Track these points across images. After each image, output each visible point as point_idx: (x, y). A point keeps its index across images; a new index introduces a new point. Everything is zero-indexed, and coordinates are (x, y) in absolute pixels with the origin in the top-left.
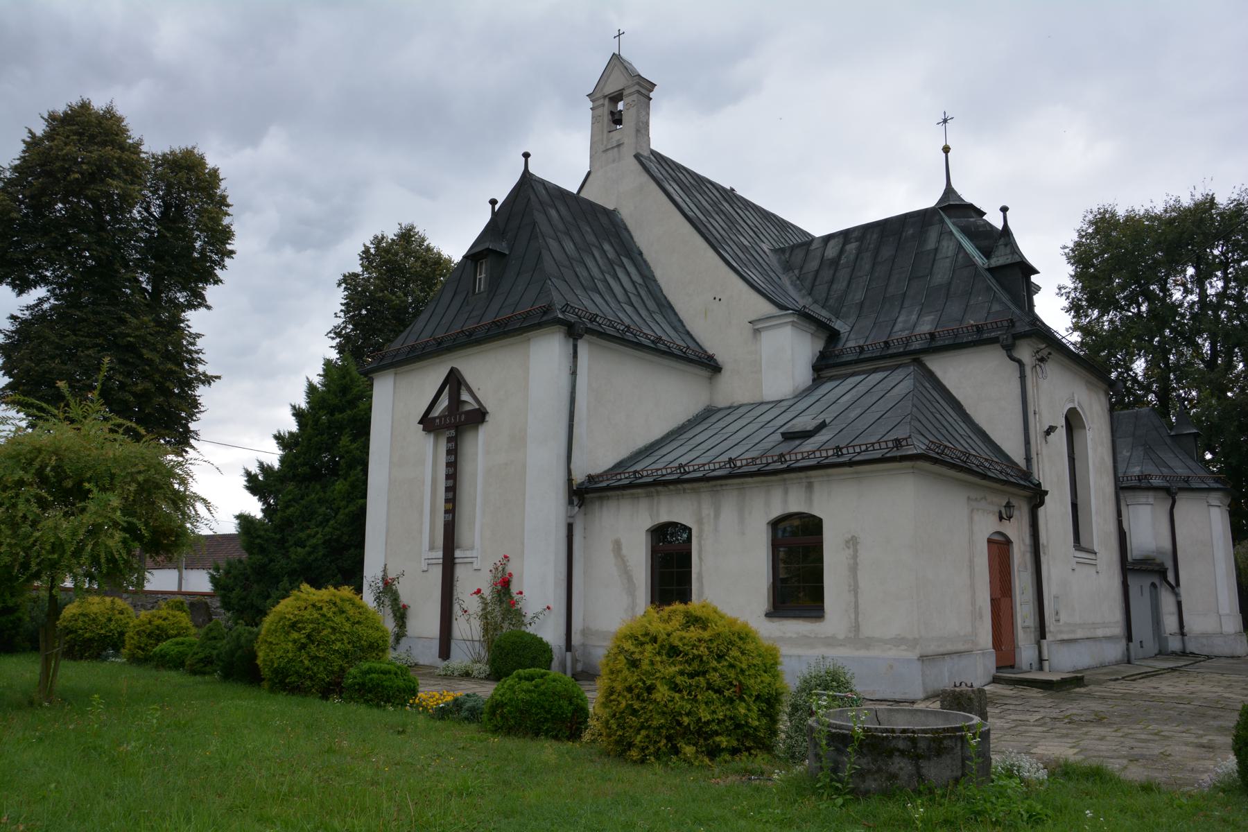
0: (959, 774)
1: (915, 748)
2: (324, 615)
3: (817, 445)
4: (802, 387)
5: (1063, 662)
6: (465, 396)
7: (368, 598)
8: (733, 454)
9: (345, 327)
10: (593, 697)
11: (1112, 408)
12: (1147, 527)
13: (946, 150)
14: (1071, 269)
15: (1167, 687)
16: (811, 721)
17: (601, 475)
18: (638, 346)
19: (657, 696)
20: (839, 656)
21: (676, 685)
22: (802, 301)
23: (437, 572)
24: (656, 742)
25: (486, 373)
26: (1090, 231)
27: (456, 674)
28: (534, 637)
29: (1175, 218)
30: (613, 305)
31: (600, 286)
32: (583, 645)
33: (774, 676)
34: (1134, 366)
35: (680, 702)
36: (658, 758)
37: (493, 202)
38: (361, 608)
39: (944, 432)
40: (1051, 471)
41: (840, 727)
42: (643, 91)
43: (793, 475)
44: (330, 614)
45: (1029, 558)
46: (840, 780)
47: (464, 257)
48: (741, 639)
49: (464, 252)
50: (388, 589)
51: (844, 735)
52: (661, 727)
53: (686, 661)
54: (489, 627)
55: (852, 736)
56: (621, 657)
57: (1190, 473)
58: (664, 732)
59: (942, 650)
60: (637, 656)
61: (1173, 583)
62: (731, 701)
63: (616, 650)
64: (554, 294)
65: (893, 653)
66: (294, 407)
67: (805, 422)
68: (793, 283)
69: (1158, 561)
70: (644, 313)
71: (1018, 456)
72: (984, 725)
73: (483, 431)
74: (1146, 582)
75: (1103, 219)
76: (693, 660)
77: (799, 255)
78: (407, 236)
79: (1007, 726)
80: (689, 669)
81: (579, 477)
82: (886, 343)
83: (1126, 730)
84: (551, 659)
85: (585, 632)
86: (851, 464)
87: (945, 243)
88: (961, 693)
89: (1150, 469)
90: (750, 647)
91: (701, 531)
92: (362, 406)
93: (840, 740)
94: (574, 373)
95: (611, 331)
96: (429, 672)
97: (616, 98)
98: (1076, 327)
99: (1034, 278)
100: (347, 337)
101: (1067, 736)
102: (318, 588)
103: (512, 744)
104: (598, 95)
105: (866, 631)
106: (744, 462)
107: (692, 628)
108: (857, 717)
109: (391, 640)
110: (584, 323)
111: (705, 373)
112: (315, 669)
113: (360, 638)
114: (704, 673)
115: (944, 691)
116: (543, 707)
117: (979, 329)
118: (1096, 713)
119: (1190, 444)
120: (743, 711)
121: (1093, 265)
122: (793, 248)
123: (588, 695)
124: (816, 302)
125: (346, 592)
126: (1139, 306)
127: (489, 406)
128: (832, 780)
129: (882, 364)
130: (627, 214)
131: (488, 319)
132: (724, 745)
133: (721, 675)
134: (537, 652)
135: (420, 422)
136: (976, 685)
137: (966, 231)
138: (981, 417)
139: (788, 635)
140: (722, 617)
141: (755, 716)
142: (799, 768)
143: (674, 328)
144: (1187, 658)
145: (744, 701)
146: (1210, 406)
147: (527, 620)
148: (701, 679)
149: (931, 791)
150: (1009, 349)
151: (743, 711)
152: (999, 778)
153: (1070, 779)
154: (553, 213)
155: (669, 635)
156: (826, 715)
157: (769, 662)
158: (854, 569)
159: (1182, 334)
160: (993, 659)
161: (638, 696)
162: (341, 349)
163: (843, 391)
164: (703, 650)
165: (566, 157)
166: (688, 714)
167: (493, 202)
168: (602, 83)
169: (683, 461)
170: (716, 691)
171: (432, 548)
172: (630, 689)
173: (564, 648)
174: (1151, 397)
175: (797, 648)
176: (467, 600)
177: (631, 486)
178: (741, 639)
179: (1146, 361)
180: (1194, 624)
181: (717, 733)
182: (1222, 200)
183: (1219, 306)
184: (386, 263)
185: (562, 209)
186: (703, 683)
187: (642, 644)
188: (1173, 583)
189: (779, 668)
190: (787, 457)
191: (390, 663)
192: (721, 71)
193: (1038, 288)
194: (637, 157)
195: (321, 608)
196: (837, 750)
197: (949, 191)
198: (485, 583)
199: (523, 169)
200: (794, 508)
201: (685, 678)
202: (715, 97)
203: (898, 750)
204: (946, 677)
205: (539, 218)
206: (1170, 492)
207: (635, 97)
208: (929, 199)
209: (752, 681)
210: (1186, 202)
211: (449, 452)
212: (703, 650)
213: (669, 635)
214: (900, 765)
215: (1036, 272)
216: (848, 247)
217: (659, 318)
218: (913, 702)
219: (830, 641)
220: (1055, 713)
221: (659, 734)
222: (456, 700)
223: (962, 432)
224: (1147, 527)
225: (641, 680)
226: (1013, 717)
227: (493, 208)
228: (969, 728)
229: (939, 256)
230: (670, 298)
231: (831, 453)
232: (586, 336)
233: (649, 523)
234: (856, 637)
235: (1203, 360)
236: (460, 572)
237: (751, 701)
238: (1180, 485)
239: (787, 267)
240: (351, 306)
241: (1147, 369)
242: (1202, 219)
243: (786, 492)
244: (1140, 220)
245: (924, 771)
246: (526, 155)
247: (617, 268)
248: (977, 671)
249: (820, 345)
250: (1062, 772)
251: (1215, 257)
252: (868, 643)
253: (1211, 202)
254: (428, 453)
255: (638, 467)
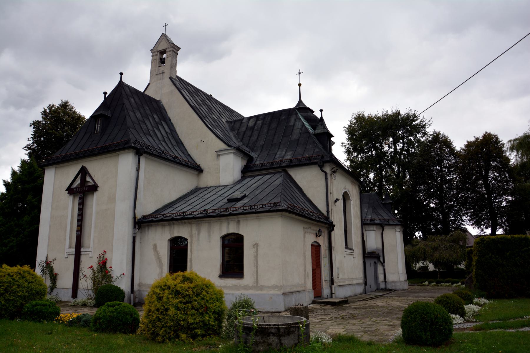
0: (297, 342)
1: (279, 332)
2: (14, 279)
3: (242, 204)
4: (237, 180)
5: (341, 294)
6: (88, 179)
7: (38, 271)
8: (207, 207)
9: (33, 145)
10: (142, 314)
11: (361, 192)
12: (373, 240)
13: (300, 85)
14: (346, 136)
15: (379, 303)
16: (236, 322)
17: (148, 216)
18: (167, 160)
19: (170, 313)
20: (249, 294)
21: (178, 308)
22: (238, 144)
23: (72, 258)
24: (169, 333)
25: (99, 169)
26: (354, 121)
27: (80, 304)
28: (116, 287)
29: (386, 118)
30: (157, 142)
31: (151, 133)
32: (139, 291)
33: (221, 303)
34: (370, 176)
35: (180, 315)
36: (170, 340)
37: (105, 93)
38: (34, 276)
39: (294, 200)
40: (337, 217)
41: (248, 324)
42: (175, 50)
43: (232, 217)
44: (17, 279)
45: (327, 252)
46: (248, 347)
47: (91, 117)
48: (207, 287)
49: (91, 114)
50: (48, 266)
51: (249, 327)
52: (172, 326)
53: (183, 297)
54: (96, 282)
55: (253, 328)
56: (154, 296)
57: (389, 219)
58: (173, 328)
59: (292, 290)
60: (161, 295)
61: (382, 261)
62: (202, 314)
63: (152, 293)
64: (131, 135)
65: (272, 292)
66: (4, 181)
67: (238, 195)
68: (234, 136)
69: (377, 253)
70: (170, 146)
71: (323, 210)
72: (307, 321)
73: (96, 195)
74: (372, 261)
75: (359, 117)
76: (186, 296)
77: (237, 125)
78: (65, 105)
79: (318, 321)
80: (184, 300)
81: (139, 216)
82: (272, 163)
83: (363, 321)
84: (124, 297)
85: (140, 285)
86: (256, 213)
87: (297, 123)
88: (298, 308)
89: (375, 217)
90: (211, 290)
91: (192, 240)
92: (39, 182)
93: (248, 329)
94: (138, 170)
95: (155, 153)
96: (66, 304)
97: (163, 52)
98: (348, 159)
99: (332, 139)
100: (33, 150)
101: (340, 324)
102: (12, 266)
103: (104, 336)
104: (155, 50)
105: (261, 283)
106: (211, 211)
107: (186, 283)
108: (255, 320)
109: (48, 290)
110: (143, 149)
111: (196, 173)
112: (8, 305)
113: (32, 290)
114: (190, 302)
115: (291, 308)
116: (119, 319)
117: (310, 158)
118: (352, 314)
119: (389, 207)
120: (207, 318)
121: (355, 135)
122: (235, 121)
123: (140, 313)
124: (244, 144)
125: (26, 268)
126: (372, 152)
127: (99, 183)
128: (244, 347)
129: (270, 171)
130: (165, 103)
131: (100, 145)
132: (199, 333)
133: (198, 303)
134: (118, 294)
135: (66, 190)
136: (305, 305)
137: (306, 118)
138: (309, 195)
139: (228, 285)
140: (199, 278)
141: (212, 320)
142: (231, 342)
143: (183, 153)
144: (387, 291)
145: (208, 314)
146: (397, 192)
147: (113, 280)
148: (189, 305)
149: (285, 350)
150: (321, 167)
151: (207, 318)
152: (313, 343)
153: (341, 342)
154: (132, 100)
155: (175, 286)
156: (243, 319)
157: (219, 296)
158: (256, 257)
159: (387, 164)
160: (313, 294)
161: (162, 313)
162: (30, 155)
163: (253, 182)
164: (190, 292)
165: (139, 76)
166: (183, 320)
167: (105, 93)
168: (158, 43)
169: (185, 210)
170: (196, 310)
171: (70, 247)
172: (158, 310)
173: (130, 292)
174: (376, 188)
175: (231, 291)
176: (86, 270)
177: (162, 220)
178: (207, 287)
179: (374, 174)
180: (390, 278)
181: (196, 328)
182: (403, 113)
183: (401, 154)
184: (54, 117)
185: (136, 99)
186: (190, 307)
187: (164, 290)
188: (382, 261)
189: (223, 299)
190: (229, 209)
191: (47, 300)
192: (212, 46)
193: (334, 143)
194: (171, 78)
195: (13, 276)
196: (247, 334)
197: (300, 102)
198: (95, 263)
199: (119, 80)
200: (232, 231)
201: (182, 304)
202: (212, 56)
203: (272, 333)
204: (293, 302)
205: (126, 101)
206: (382, 226)
207: (171, 52)
208: (292, 104)
209: (212, 305)
210: (390, 113)
211: (80, 204)
212: (190, 292)
213: (175, 286)
214: (273, 339)
215: (333, 136)
216: (258, 122)
217: (176, 148)
218: (280, 312)
219: (246, 288)
220: (336, 315)
221: (170, 330)
222: (78, 317)
223: (302, 200)
224: (373, 240)
225: (163, 306)
226: (320, 317)
227: (105, 96)
228: (301, 323)
229: (295, 128)
230: (182, 140)
231: (247, 208)
232: (144, 155)
233: (169, 237)
234: (257, 286)
235: (395, 174)
236: (83, 258)
237: (211, 314)
238: (386, 223)
239: (232, 129)
240: (36, 136)
241: (374, 177)
242: (395, 120)
243: (228, 224)
244: (373, 119)
245: (283, 341)
246: (121, 74)
247: (159, 126)
248: (306, 299)
249: (245, 163)
250: (338, 339)
251: (400, 134)
252: (262, 288)
253: (398, 114)
254: (70, 204)
255: (165, 212)
